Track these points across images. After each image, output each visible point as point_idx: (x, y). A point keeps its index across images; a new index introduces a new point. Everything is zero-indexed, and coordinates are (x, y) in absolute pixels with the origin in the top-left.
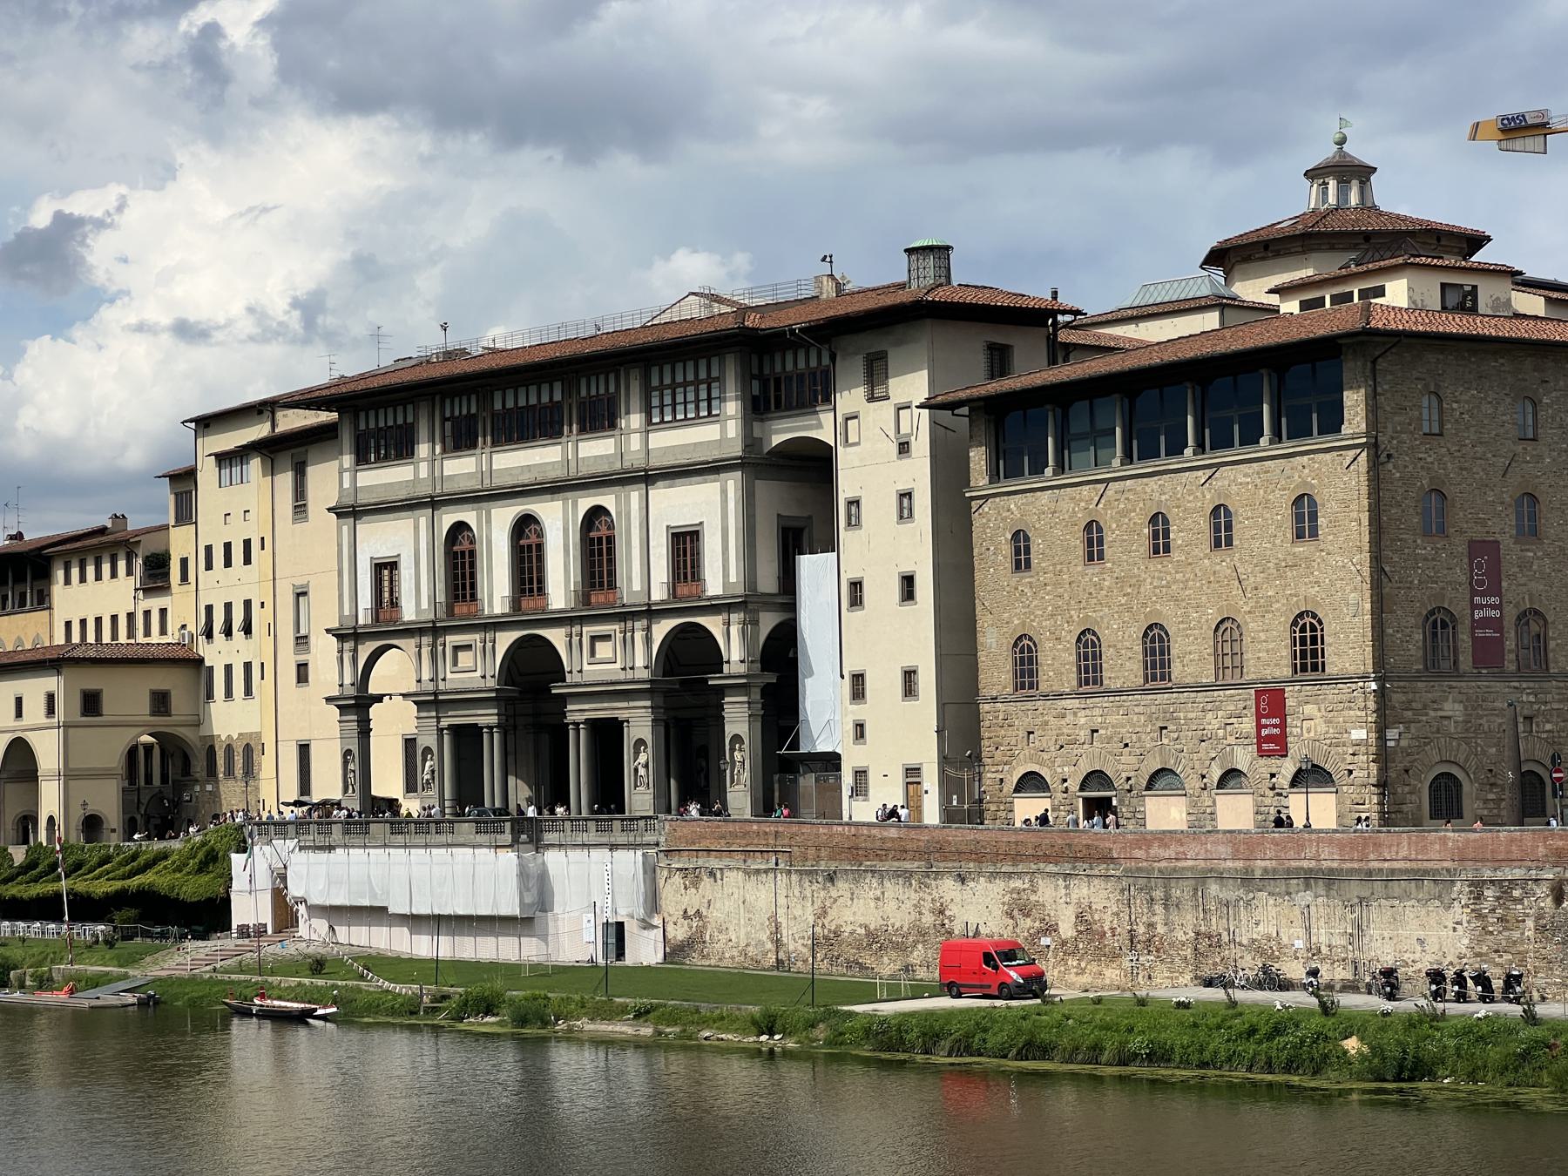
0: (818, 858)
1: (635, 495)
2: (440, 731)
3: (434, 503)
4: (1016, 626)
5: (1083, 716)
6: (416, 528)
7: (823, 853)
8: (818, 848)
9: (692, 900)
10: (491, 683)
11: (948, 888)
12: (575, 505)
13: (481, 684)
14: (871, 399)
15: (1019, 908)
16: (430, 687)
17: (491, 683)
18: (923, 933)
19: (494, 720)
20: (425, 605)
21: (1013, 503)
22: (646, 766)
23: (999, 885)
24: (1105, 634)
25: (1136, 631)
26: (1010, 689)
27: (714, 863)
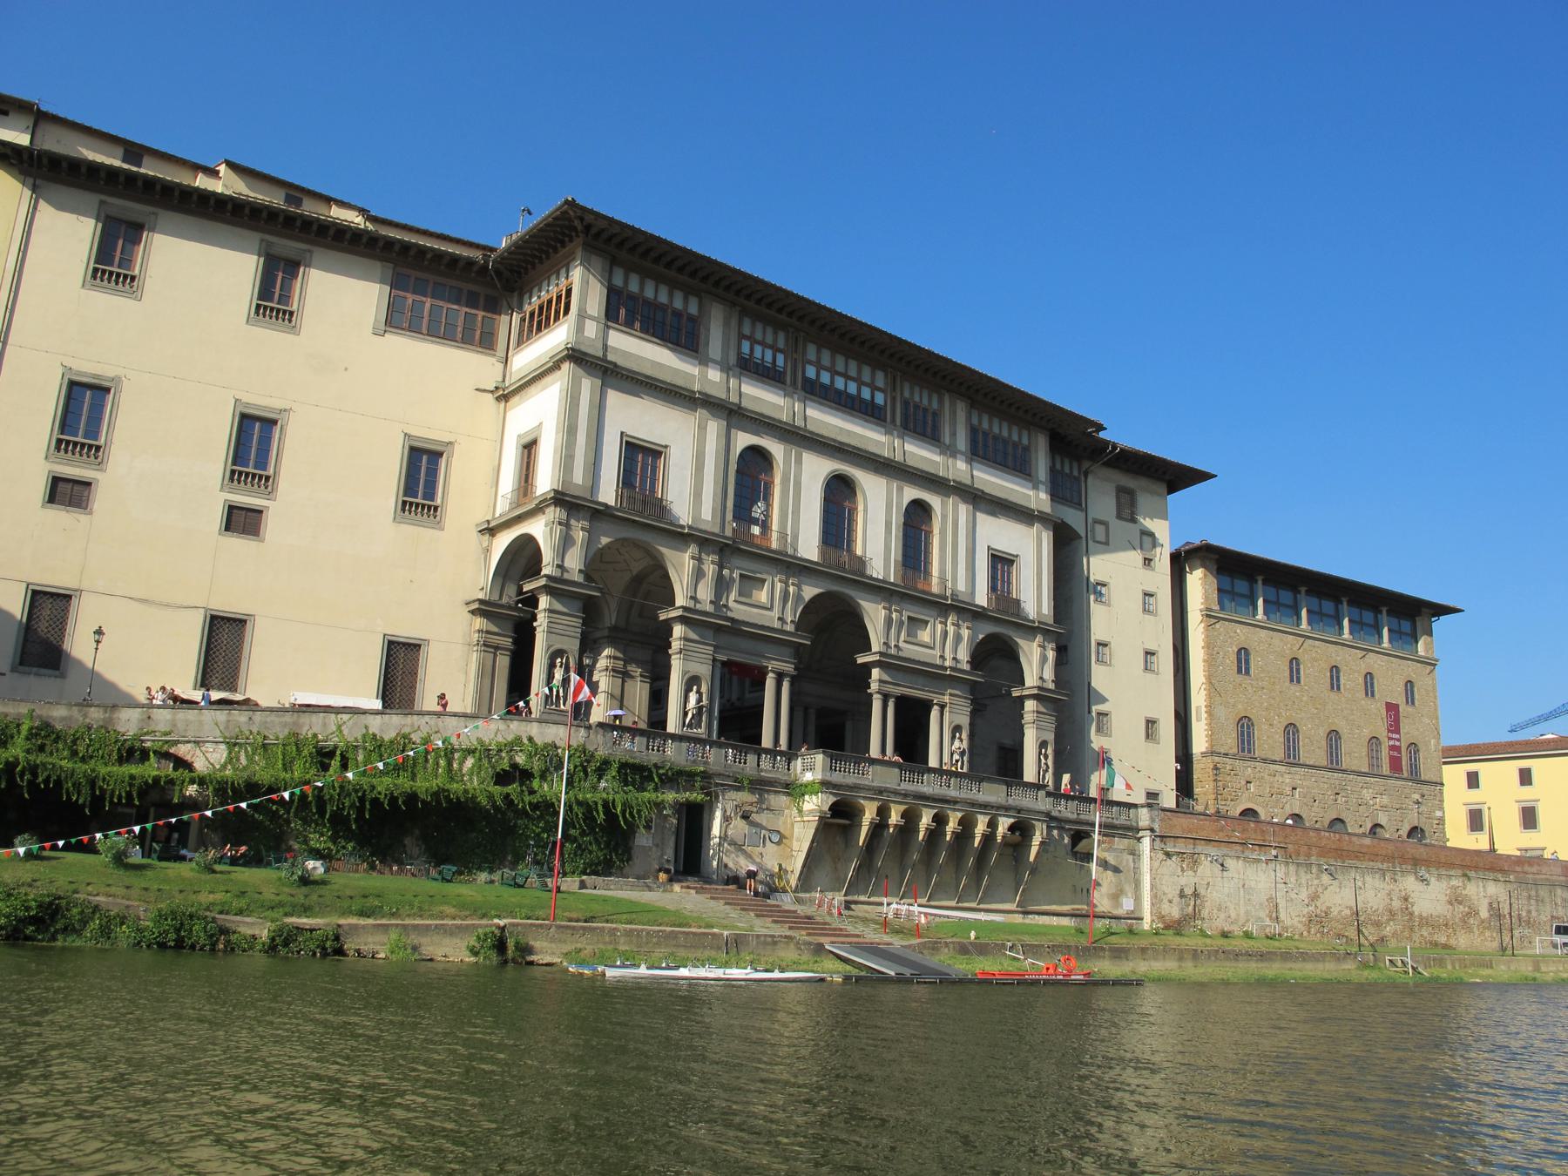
0: (1309, 856)
1: (964, 509)
2: (714, 660)
3: (734, 414)
4: (1241, 710)
5: (1286, 777)
6: (702, 428)
7: (1314, 851)
8: (1309, 847)
9: (1188, 880)
10: (790, 628)
11: (1409, 883)
12: (900, 490)
13: (777, 625)
14: (1119, 517)
15: (1456, 899)
16: (709, 608)
17: (790, 628)
18: (1392, 914)
19: (789, 668)
20: (707, 513)
21: (1239, 629)
22: (962, 754)
23: (1444, 885)
24: (1303, 728)
25: (1323, 732)
26: (1235, 750)
27: (1213, 851)
